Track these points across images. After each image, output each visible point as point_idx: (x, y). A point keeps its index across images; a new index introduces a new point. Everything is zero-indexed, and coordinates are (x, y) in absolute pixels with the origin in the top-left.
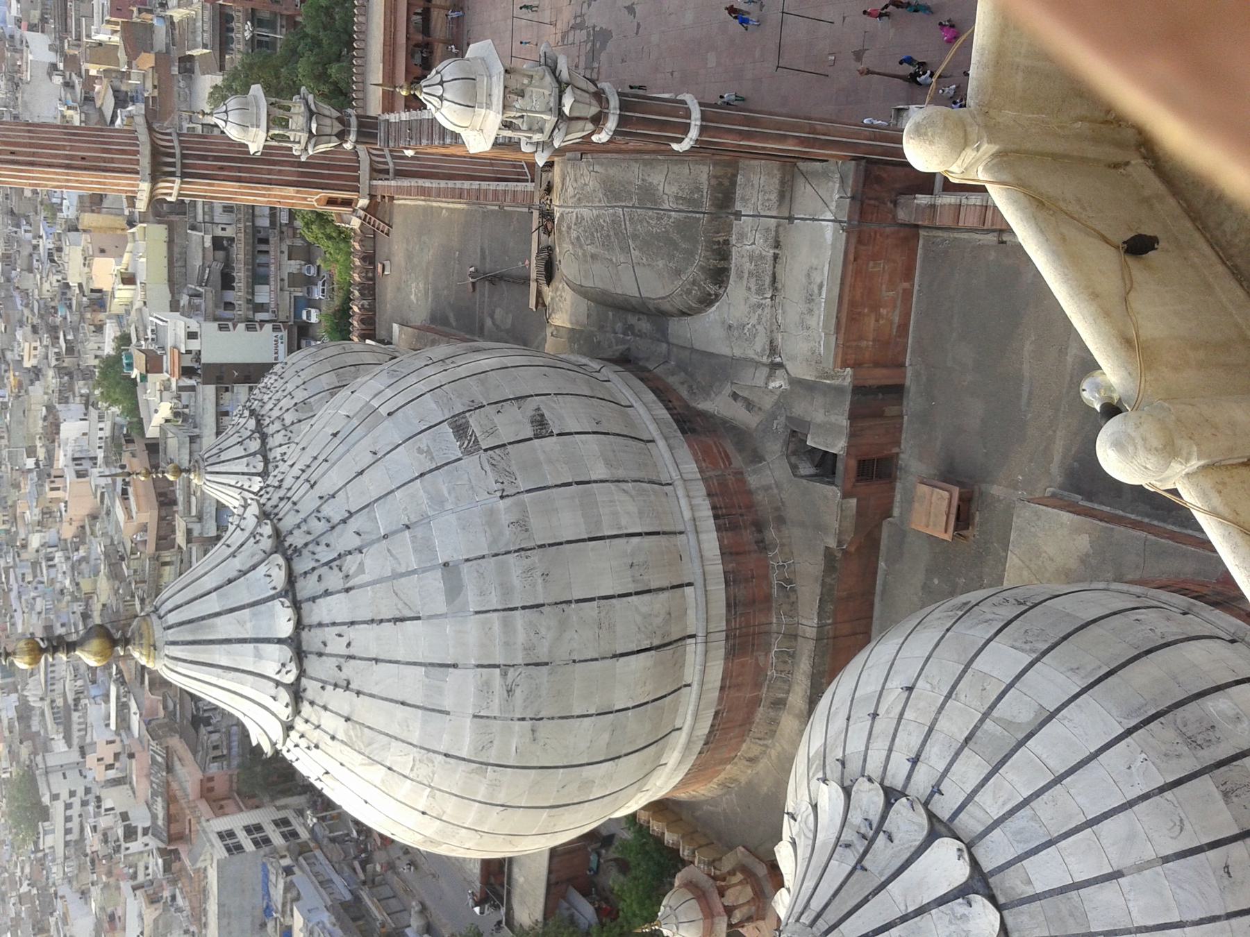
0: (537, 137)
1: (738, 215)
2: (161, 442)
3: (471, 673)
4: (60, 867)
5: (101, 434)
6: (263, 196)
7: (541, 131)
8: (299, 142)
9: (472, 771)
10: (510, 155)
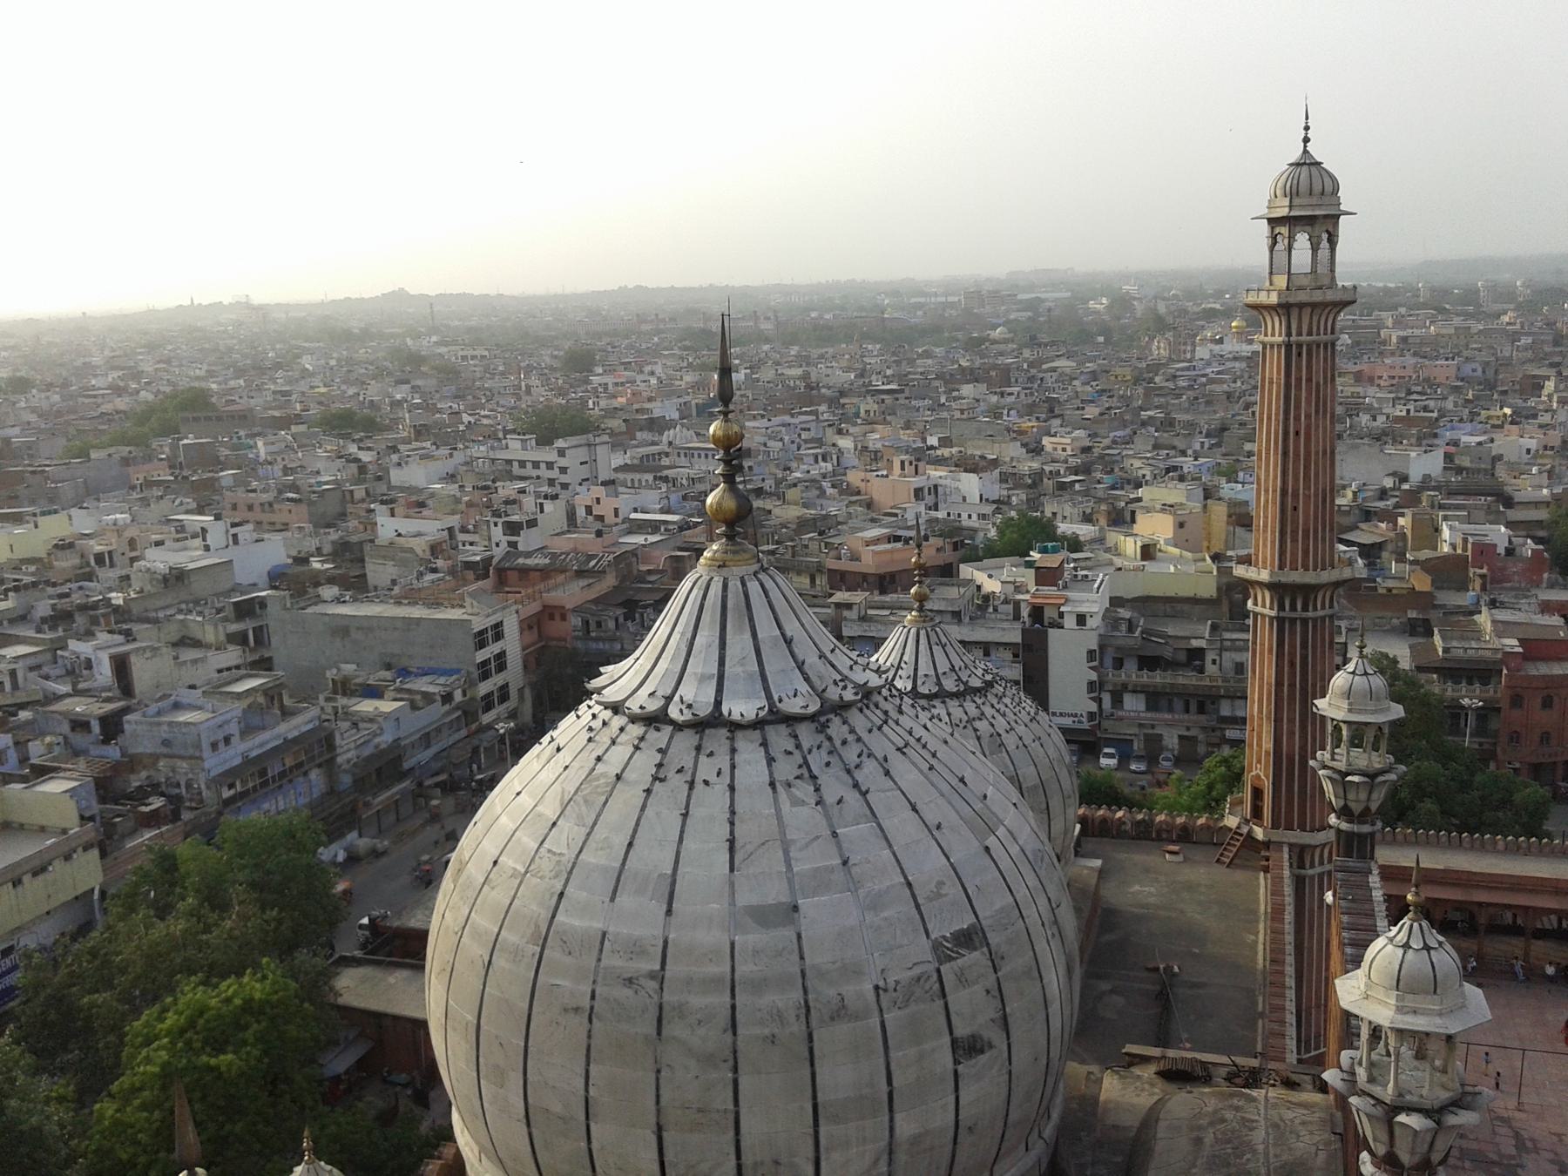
0: (1361, 1073)
2: (954, 580)
3: (659, 932)
7: (1371, 1080)
8: (1333, 759)
9: (537, 926)
10: (1333, 1033)
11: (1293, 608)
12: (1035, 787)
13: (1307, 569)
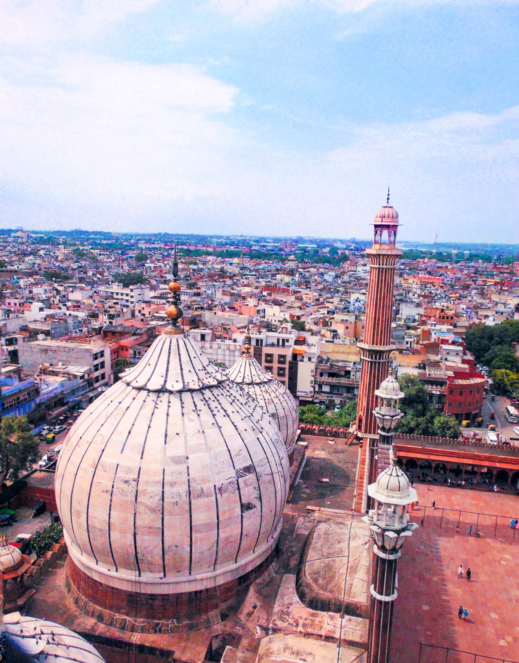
1: (342, 617)
5: (274, 321)
11: (376, 358)
12: (283, 417)
13: (381, 345)
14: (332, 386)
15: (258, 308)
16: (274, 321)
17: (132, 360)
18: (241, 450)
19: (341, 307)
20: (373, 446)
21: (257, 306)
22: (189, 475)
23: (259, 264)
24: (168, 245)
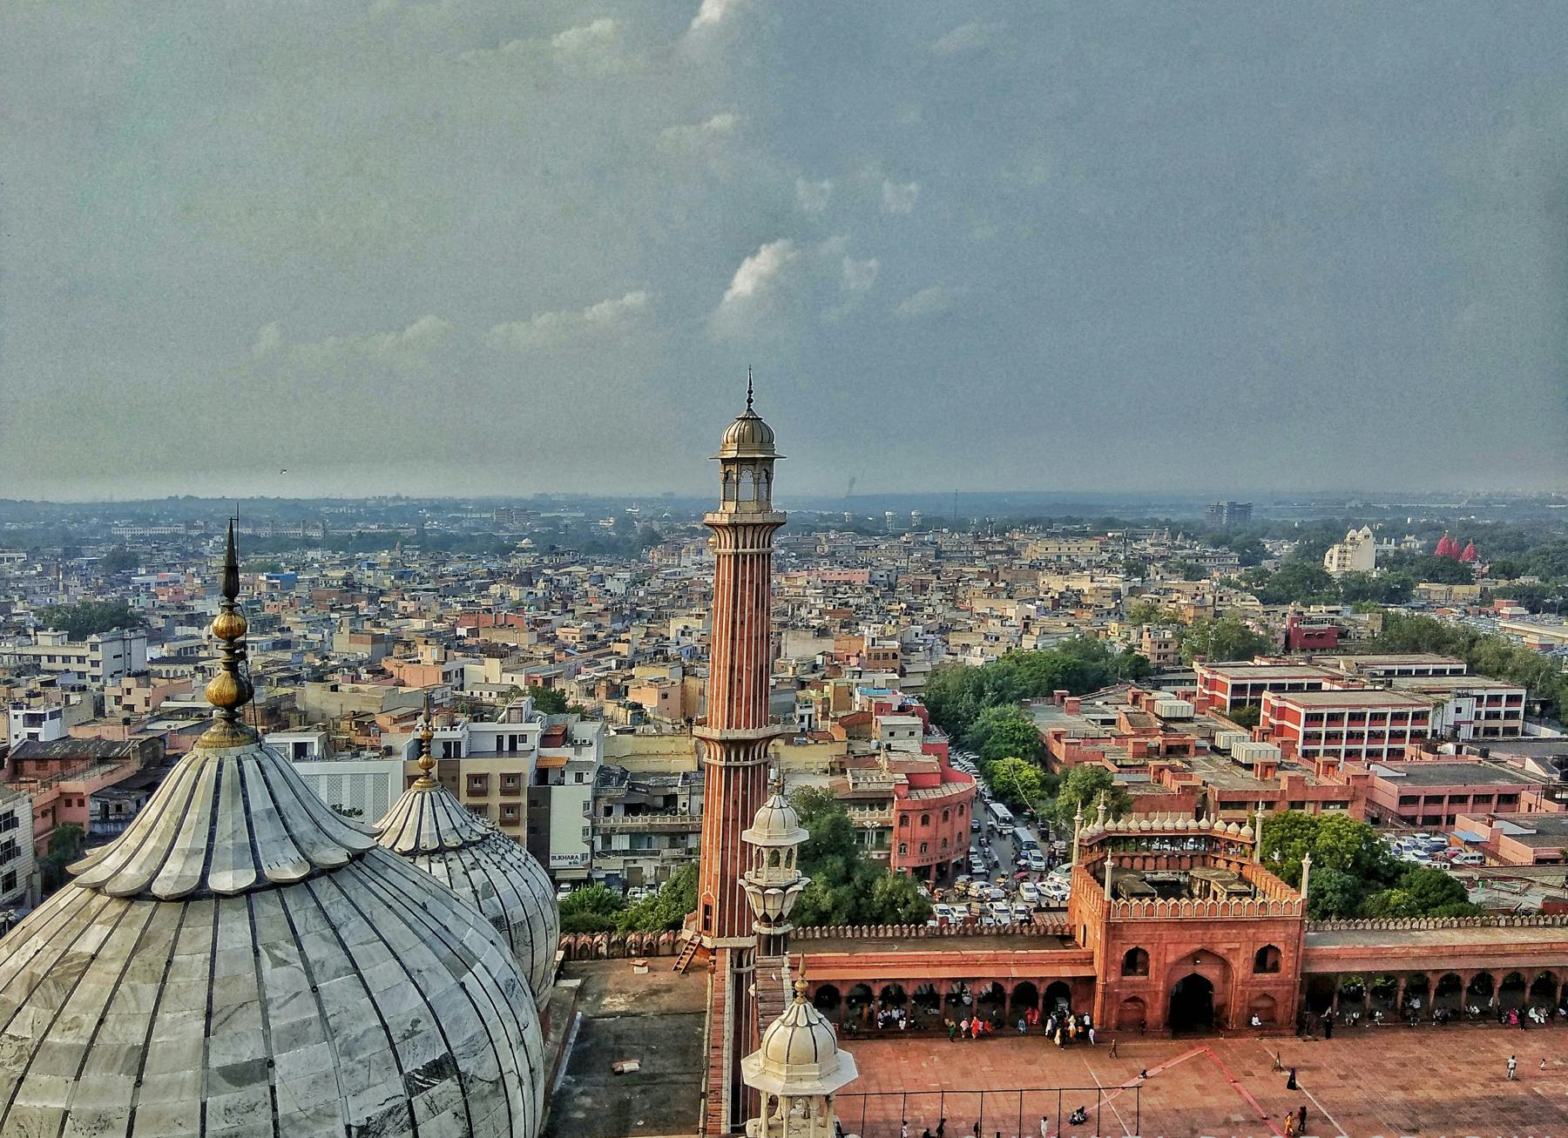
4: (11, 651)
5: (486, 694)
6: (711, 843)
14: (636, 836)
15: (446, 668)
16: (486, 694)
17: (98, 829)
18: (417, 1021)
19: (648, 648)
20: (740, 965)
21: (443, 663)
22: (275, 1109)
23: (444, 563)
24: (195, 528)
